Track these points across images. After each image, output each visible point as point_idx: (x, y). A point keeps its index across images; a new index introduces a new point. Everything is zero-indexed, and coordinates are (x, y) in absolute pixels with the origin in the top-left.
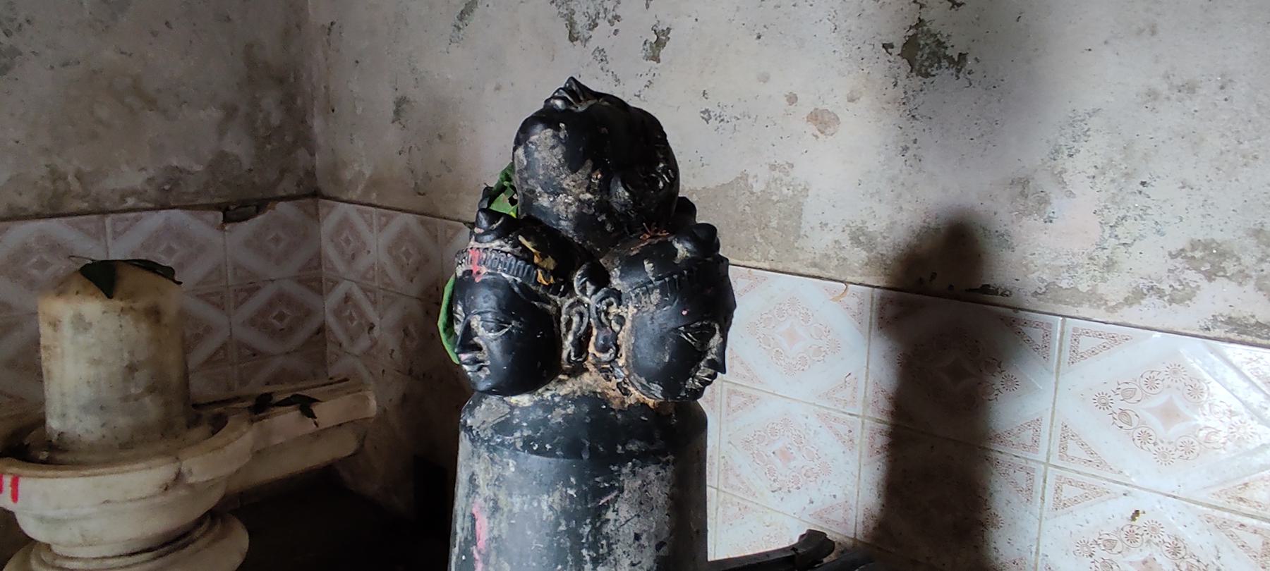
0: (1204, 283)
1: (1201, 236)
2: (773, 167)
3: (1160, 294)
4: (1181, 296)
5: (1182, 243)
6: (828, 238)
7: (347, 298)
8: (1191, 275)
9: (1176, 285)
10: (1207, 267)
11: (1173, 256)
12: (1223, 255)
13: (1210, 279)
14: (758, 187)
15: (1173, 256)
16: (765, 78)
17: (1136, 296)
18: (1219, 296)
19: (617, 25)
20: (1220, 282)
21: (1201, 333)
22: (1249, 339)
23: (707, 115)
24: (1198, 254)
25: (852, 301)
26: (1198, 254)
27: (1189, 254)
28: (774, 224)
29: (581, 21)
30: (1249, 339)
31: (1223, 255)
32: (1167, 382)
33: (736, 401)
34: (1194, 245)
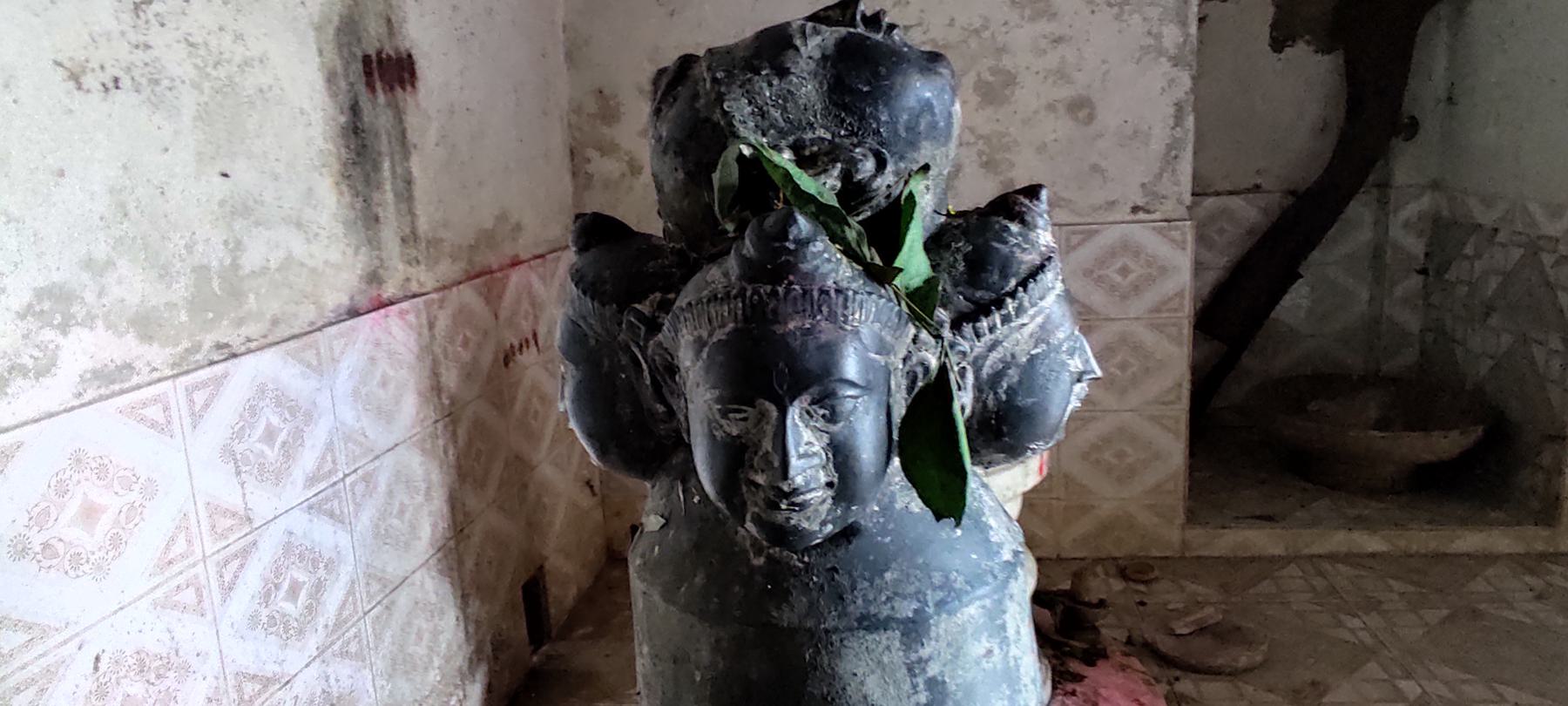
0: (60, 340)
1: (41, 282)
3: (23, 371)
4: (44, 369)
5: (27, 297)
8: (48, 334)
9: (36, 353)
10: (58, 319)
11: (22, 316)
13: (65, 333)
15: (22, 316)
18: (82, 350)
20: (76, 330)
21: (76, 403)
22: (117, 387)
24: (46, 306)
26: (46, 306)
27: (37, 309)
30: (117, 387)
32: (76, 477)
34: (40, 294)
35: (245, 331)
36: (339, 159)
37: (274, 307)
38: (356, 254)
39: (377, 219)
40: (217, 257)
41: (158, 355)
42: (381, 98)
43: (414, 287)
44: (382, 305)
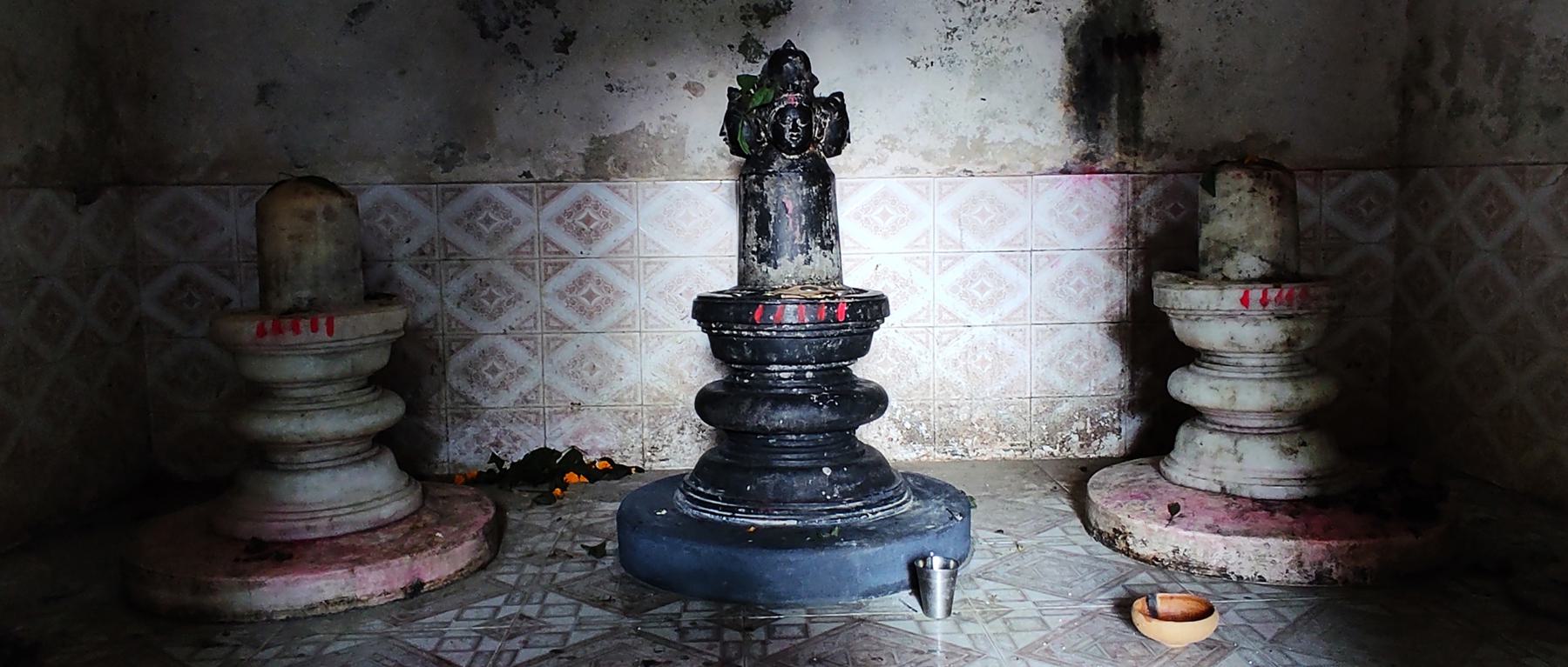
2: (663, 118)
7: (184, 281)
12: (895, 140)
14: (652, 132)
16: (653, 64)
17: (864, 165)
18: (896, 159)
19: (527, 28)
23: (610, 88)
25: (724, 191)
28: (666, 152)
29: (491, 23)
31: (895, 140)
33: (650, 269)
35: (982, 168)
36: (1071, 93)
38: (1076, 141)
39: (1099, 126)
40: (971, 132)
41: (932, 167)
43: (1130, 167)
44: (1092, 172)
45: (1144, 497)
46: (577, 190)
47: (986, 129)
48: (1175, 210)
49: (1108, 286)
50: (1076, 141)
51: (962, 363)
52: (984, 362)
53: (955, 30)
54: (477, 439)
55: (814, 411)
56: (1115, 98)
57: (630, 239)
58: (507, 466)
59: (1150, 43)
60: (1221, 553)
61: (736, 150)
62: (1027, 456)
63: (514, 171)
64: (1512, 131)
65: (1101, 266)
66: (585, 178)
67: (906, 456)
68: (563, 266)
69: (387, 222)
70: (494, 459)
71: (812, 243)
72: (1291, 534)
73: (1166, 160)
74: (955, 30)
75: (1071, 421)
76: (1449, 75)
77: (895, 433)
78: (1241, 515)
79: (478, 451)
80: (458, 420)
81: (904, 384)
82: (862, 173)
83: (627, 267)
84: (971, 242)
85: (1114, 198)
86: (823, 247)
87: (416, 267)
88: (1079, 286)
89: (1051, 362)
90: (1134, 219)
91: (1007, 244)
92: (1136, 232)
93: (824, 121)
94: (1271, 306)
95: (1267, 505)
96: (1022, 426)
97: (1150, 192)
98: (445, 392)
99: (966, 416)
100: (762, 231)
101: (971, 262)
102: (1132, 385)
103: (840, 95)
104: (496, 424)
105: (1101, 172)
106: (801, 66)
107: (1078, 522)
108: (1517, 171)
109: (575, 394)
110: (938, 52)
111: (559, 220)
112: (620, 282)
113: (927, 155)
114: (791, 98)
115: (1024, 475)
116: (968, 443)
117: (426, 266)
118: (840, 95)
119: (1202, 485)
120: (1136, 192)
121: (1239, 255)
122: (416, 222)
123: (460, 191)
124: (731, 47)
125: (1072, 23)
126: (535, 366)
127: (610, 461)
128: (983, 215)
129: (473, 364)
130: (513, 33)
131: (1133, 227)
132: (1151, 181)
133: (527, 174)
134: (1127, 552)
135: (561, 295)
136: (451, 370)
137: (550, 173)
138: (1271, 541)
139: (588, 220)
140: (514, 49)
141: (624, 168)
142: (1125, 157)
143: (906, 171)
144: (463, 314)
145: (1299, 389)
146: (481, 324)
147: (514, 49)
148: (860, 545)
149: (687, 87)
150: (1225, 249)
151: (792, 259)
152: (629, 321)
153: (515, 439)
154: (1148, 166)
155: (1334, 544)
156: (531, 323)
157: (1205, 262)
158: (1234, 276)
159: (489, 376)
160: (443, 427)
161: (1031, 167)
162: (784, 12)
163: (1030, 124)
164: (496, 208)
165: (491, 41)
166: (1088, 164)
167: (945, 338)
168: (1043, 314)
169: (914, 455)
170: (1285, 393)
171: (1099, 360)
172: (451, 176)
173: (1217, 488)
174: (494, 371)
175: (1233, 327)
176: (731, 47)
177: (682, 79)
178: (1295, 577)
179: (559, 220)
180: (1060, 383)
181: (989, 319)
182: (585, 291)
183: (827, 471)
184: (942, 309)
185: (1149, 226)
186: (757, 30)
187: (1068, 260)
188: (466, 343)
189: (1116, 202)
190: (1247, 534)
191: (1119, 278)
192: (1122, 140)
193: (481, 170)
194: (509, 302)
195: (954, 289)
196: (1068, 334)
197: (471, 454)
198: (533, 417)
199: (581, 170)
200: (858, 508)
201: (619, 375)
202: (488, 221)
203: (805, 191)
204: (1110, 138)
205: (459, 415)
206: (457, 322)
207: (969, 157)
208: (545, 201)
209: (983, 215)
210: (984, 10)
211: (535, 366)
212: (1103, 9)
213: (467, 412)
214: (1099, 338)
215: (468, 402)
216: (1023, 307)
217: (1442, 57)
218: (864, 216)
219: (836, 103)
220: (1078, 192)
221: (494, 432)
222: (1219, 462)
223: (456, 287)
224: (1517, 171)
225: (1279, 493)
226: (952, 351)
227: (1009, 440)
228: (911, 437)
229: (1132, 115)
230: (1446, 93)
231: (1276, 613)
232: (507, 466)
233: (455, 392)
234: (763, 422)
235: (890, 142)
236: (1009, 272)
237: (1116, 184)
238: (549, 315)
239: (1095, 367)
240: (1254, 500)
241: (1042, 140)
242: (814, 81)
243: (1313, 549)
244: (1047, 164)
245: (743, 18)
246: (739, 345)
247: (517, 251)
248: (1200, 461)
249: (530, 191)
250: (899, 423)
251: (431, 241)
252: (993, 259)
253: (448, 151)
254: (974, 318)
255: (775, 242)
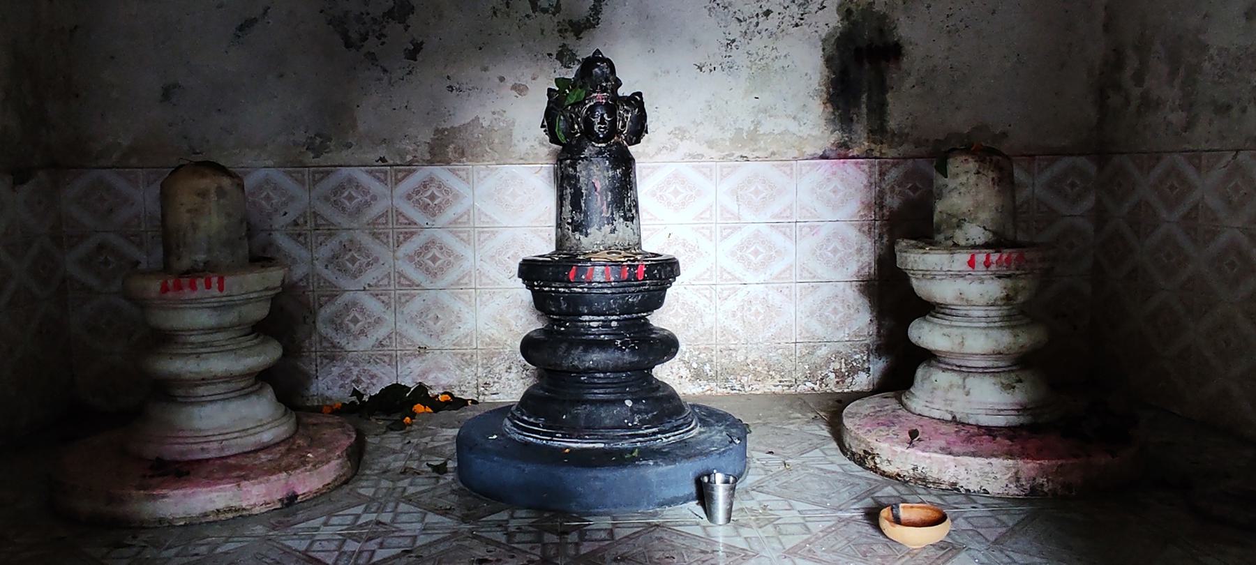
2: (494, 113)
4: (673, 149)
6: (527, 144)
16: (486, 69)
18: (685, 147)
19: (383, 39)
25: (544, 172)
28: (497, 141)
29: (354, 36)
35: (756, 154)
36: (828, 93)
37: (774, 148)
38: (832, 132)
39: (852, 120)
40: (747, 125)
41: (714, 154)
42: (867, 66)
44: (846, 157)
45: (889, 424)
46: (423, 172)
47: (759, 123)
48: (914, 189)
49: (859, 251)
50: (832, 132)
51: (739, 314)
52: (757, 313)
53: (734, 41)
54: (342, 376)
55: (618, 354)
56: (864, 98)
57: (467, 212)
58: (366, 398)
59: (893, 51)
60: (952, 470)
61: (554, 139)
62: (792, 390)
63: (372, 157)
64: (1189, 125)
65: (853, 234)
66: (431, 163)
67: (694, 391)
68: (412, 234)
69: (268, 198)
70: (355, 392)
71: (616, 216)
72: (1010, 455)
73: (906, 148)
74: (734, 41)
75: (829, 361)
76: (1139, 78)
77: (684, 372)
78: (968, 439)
79: (341, 386)
80: (325, 361)
81: (692, 331)
82: (658, 158)
83: (464, 236)
84: (747, 216)
85: (863, 179)
86: (626, 219)
87: (290, 236)
88: (835, 251)
89: (812, 314)
90: (881, 196)
91: (776, 216)
92: (882, 207)
93: (627, 115)
94: (993, 267)
95: (990, 431)
96: (789, 366)
97: (893, 174)
98: (315, 338)
99: (743, 358)
100: (576, 206)
101: (748, 231)
102: (879, 332)
103: (640, 94)
104: (356, 365)
105: (853, 157)
106: (607, 71)
107: (834, 445)
108: (1194, 157)
109: (422, 340)
110: (720, 60)
111: (409, 197)
112: (458, 247)
113: (711, 144)
114: (600, 97)
115: (790, 406)
116: (744, 380)
117: (300, 235)
118: (640, 94)
119: (937, 414)
120: (882, 174)
121: (966, 225)
122: (292, 199)
123: (328, 173)
124: (550, 55)
125: (830, 35)
126: (389, 317)
127: (450, 394)
128: (757, 192)
129: (339, 315)
130: (372, 44)
131: (879, 202)
132: (894, 165)
133: (383, 160)
134: (875, 469)
135: (410, 258)
136: (319, 319)
137: (402, 158)
138: (993, 460)
139: (433, 197)
140: (372, 57)
141: (463, 154)
142: (873, 146)
143: (694, 157)
144: (329, 274)
145: (1016, 336)
146: (343, 282)
147: (372, 57)
148: (656, 464)
149: (515, 87)
150: (954, 220)
151: (600, 229)
152: (466, 280)
153: (373, 377)
154: (892, 153)
155: (1045, 462)
156: (385, 281)
157: (939, 232)
158: (963, 243)
159: (351, 325)
160: (314, 367)
161: (796, 154)
162: (593, 26)
163: (794, 118)
164: (357, 187)
165: (353, 50)
166: (842, 152)
167: (725, 293)
168: (805, 274)
169: (700, 390)
170: (1004, 339)
171: (852, 311)
172: (321, 161)
173: (949, 417)
174: (355, 321)
175: (961, 285)
176: (550, 55)
177: (510, 82)
178: (1013, 490)
179: (409, 197)
180: (820, 331)
181: (762, 278)
182: (430, 255)
183: (629, 403)
184: (723, 270)
185: (893, 202)
186: (570, 41)
187: (826, 229)
188: (332, 297)
189: (865, 182)
190: (974, 455)
191: (868, 244)
192: (871, 131)
193: (345, 155)
194: (368, 264)
195: (733, 254)
196: (826, 290)
197: (336, 389)
198: (387, 359)
199: (428, 157)
200: (654, 434)
201: (458, 324)
202: (350, 198)
203: (611, 173)
204: (861, 129)
205: (326, 357)
206: (326, 281)
207: (746, 145)
208: (398, 181)
209: (757, 192)
210: (757, 24)
211: (389, 317)
212: (854, 24)
213: (333, 354)
214: (852, 295)
215: (334, 347)
216: (789, 268)
217: (1132, 63)
218: (659, 194)
219: (636, 101)
220: (834, 174)
221: (355, 371)
222: (950, 396)
223: (324, 252)
224: (1194, 157)
225: (1000, 421)
226: (731, 305)
227: (778, 378)
228: (698, 375)
229: (879, 111)
230: (1136, 92)
231: (999, 520)
232: (366, 398)
233: (323, 338)
234: (576, 363)
235: (680, 133)
236: (778, 239)
237: (866, 167)
238: (401, 275)
239: (849, 317)
240: (979, 427)
241: (805, 131)
242: (618, 83)
243: (1027, 467)
244: (809, 150)
245: (560, 31)
246: (556, 299)
247: (374, 223)
248: (934, 394)
249: (386, 173)
250: (687, 364)
251: (304, 215)
252: (765, 229)
253: (318, 140)
254: (749, 278)
255: (586, 215)
